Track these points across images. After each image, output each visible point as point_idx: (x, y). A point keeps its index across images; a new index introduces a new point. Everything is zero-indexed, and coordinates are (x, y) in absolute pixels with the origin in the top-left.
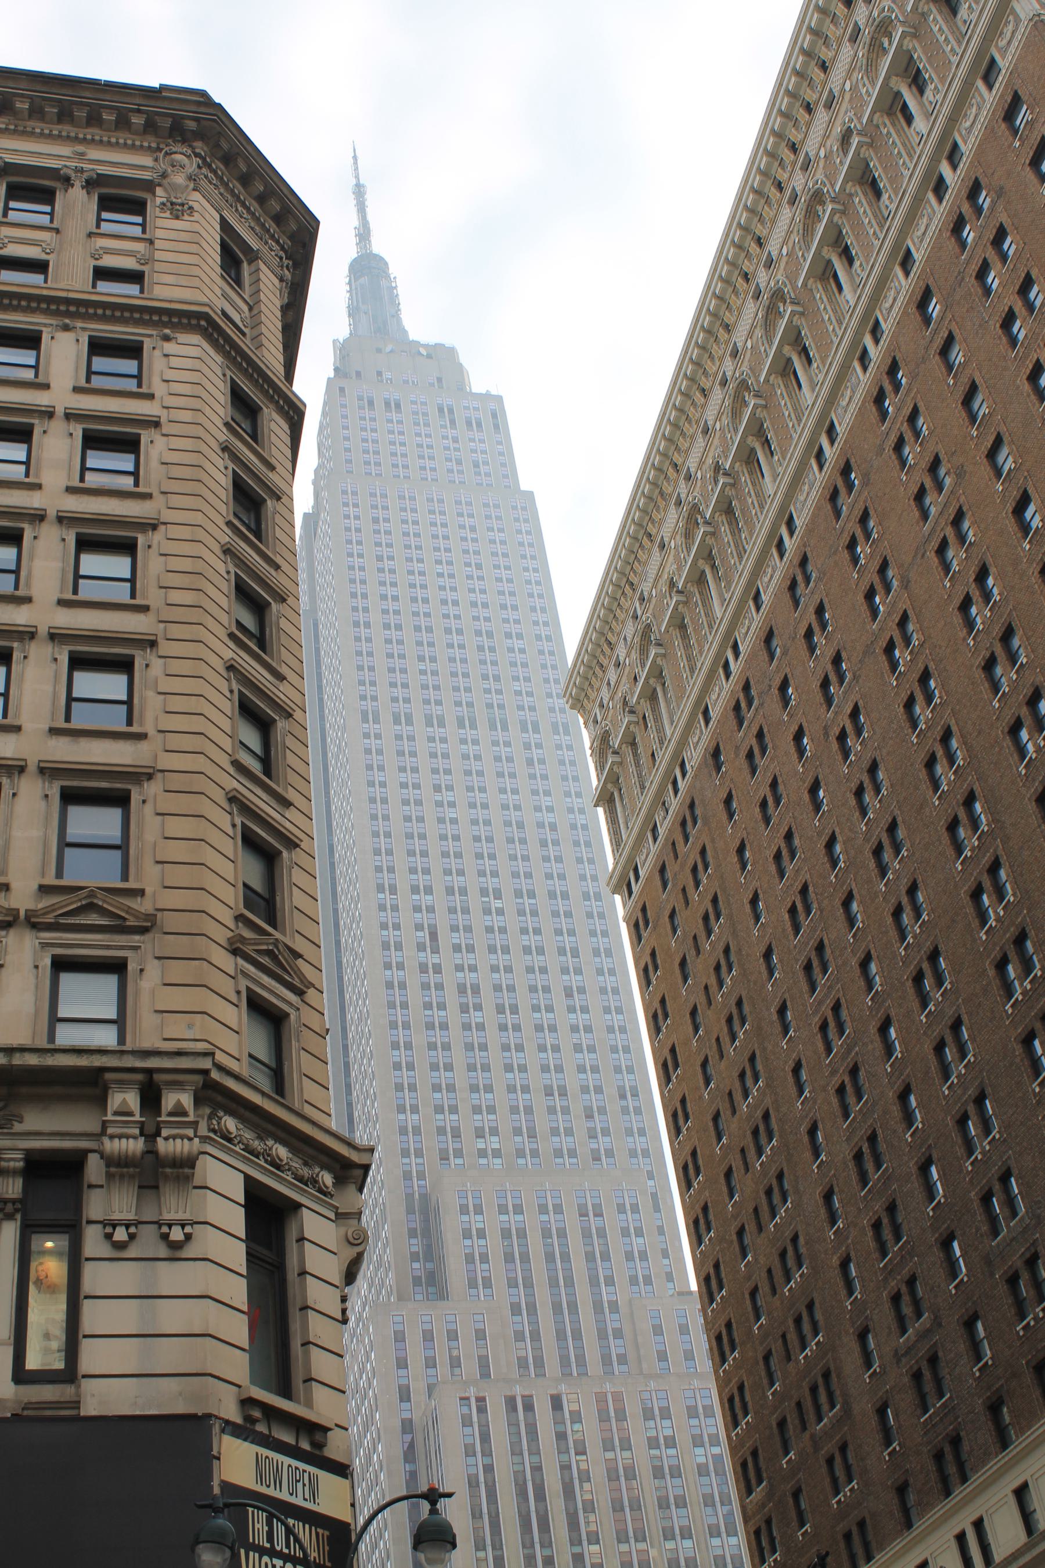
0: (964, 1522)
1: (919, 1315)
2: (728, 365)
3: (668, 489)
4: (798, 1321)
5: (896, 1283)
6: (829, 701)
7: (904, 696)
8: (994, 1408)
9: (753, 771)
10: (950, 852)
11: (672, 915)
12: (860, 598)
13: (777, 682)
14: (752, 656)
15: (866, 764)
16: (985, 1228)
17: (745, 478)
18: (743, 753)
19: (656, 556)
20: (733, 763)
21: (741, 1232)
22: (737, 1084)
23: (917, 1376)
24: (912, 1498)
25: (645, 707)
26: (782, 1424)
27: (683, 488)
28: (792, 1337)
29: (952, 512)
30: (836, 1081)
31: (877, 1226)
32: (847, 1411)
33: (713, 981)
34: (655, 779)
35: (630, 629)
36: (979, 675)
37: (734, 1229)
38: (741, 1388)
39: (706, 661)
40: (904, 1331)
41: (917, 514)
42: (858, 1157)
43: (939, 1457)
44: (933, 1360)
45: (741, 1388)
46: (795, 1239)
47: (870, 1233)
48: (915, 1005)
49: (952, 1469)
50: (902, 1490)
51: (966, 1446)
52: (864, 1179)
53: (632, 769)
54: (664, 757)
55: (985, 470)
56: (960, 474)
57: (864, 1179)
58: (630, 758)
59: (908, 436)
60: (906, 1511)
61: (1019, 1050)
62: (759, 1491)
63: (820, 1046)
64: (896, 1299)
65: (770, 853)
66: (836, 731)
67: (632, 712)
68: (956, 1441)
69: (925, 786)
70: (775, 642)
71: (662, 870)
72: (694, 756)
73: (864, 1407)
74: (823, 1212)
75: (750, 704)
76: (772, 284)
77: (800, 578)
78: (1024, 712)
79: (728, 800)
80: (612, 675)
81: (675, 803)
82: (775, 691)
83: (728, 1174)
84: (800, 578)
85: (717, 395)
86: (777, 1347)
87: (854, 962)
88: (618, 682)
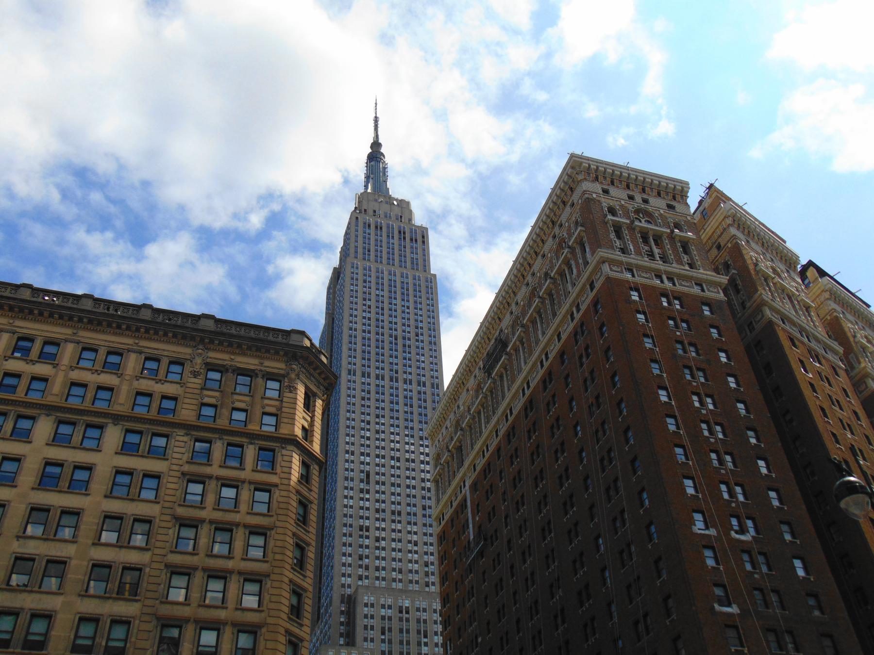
59: (551, 402)
76: (516, 313)
77: (511, 434)
84: (511, 434)
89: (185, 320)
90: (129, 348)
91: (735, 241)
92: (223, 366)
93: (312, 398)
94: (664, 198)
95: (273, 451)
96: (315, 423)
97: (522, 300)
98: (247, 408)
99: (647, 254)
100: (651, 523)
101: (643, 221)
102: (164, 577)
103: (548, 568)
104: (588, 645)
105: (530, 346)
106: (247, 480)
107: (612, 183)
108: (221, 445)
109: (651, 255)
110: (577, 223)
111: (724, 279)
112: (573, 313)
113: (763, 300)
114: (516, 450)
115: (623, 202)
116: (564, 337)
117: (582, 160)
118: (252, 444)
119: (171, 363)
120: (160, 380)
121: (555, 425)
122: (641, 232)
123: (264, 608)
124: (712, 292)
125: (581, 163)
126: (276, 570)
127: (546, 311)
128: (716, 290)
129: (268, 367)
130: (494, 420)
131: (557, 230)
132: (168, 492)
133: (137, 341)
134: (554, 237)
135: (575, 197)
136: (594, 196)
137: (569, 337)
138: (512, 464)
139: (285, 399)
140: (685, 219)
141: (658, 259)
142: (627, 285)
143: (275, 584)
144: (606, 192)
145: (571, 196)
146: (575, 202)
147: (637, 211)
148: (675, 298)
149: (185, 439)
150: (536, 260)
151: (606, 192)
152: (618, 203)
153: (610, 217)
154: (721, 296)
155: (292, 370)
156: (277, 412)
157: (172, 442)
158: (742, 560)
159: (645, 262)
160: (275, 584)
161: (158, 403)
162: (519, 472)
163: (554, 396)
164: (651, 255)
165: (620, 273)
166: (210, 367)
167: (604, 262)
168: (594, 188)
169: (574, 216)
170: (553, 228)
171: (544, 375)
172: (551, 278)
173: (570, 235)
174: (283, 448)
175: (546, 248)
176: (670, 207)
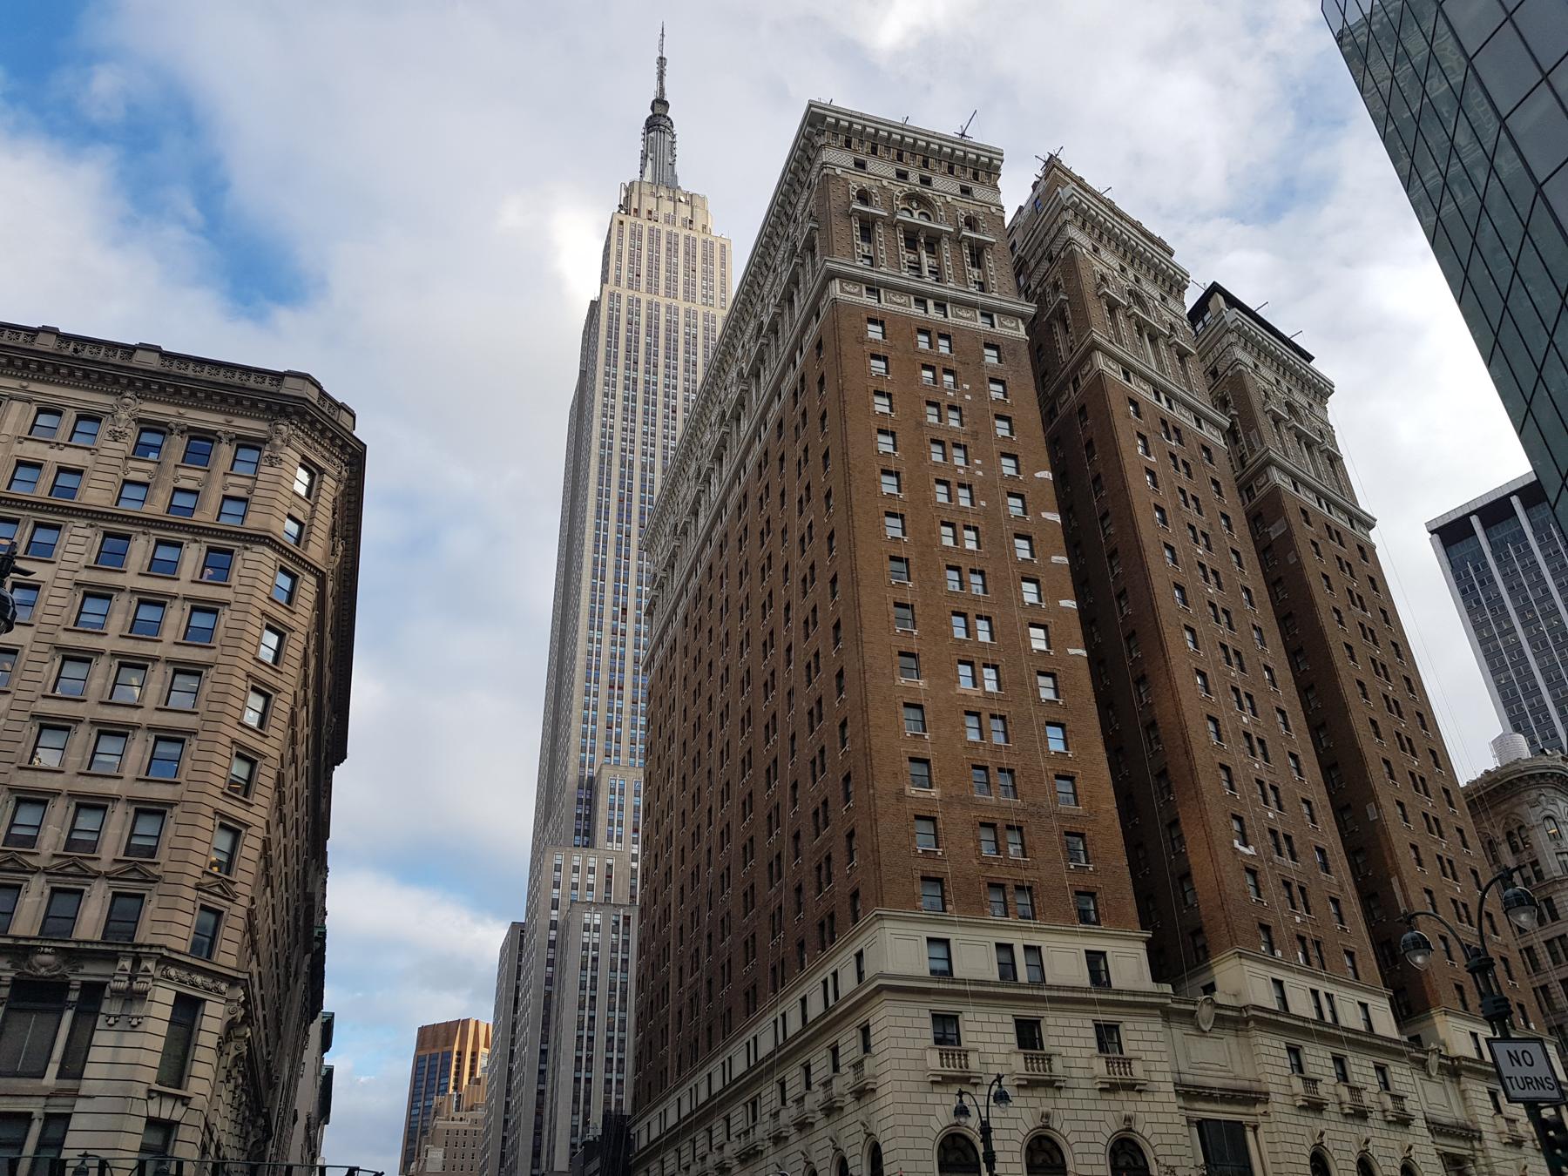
89: (111, 353)
90: (10, 394)
91: (1070, 248)
92: (165, 424)
93: (317, 477)
94: (958, 177)
95: (231, 552)
98: (198, 488)
99: (909, 267)
101: (916, 214)
102: (28, 733)
106: (181, 596)
108: (145, 542)
109: (916, 268)
111: (1030, 309)
113: (1094, 341)
115: (885, 183)
117: (826, 112)
118: (196, 541)
119: (80, 418)
120: (58, 444)
123: (182, 779)
124: (1006, 327)
125: (825, 117)
126: (209, 726)
128: (1013, 325)
132: (49, 610)
133: (25, 384)
136: (839, 171)
139: (261, 477)
140: (986, 210)
141: (927, 274)
142: (864, 316)
143: (204, 746)
144: (860, 165)
147: (909, 197)
148: (943, 336)
149: (88, 532)
151: (860, 165)
152: (878, 183)
154: (1022, 333)
155: (279, 432)
158: (963, 724)
159: (905, 278)
160: (204, 746)
161: (52, 478)
164: (916, 268)
165: (858, 295)
167: (833, 278)
168: (836, 158)
174: (247, 549)
176: (966, 191)
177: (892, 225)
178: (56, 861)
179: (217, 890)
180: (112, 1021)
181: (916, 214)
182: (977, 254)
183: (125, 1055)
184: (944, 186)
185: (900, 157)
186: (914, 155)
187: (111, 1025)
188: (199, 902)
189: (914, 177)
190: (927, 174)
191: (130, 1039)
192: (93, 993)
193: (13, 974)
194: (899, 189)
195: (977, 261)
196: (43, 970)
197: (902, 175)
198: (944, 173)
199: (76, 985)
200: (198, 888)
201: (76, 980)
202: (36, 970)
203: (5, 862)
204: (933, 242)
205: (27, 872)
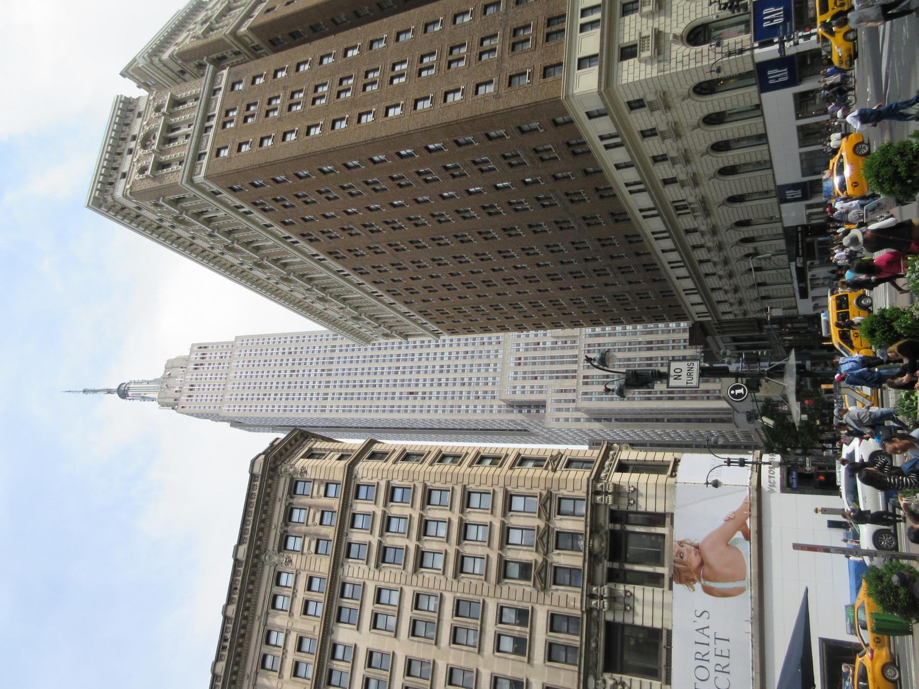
0: (668, 267)
1: (605, 270)
2: (272, 281)
3: (307, 305)
4: (596, 302)
5: (594, 275)
6: (405, 268)
7: (415, 249)
8: (638, 254)
9: (418, 292)
10: (470, 243)
11: (454, 322)
12: (376, 256)
13: (392, 282)
14: (379, 288)
15: (432, 262)
16: (586, 250)
17: (316, 282)
18: (411, 295)
19: (328, 312)
20: (413, 298)
21: (564, 314)
22: (517, 310)
23: (623, 273)
24: (658, 278)
25: (380, 321)
26: (626, 310)
27: (308, 301)
28: (601, 304)
29: (362, 227)
30: (527, 283)
31: (575, 277)
32: (626, 292)
33: (481, 313)
34: (407, 321)
35: (350, 323)
36: (419, 228)
37: (562, 316)
38: (612, 320)
39: (374, 301)
40: (609, 274)
41: (357, 237)
42: (552, 280)
43: (648, 270)
44: (620, 268)
45: (612, 320)
46: (571, 300)
47: (577, 280)
48: (513, 259)
49: (652, 267)
50: (654, 280)
51: (647, 263)
52: (561, 279)
53: (400, 328)
54: (401, 317)
55: (353, 217)
56: (350, 223)
57: (561, 279)
58: (396, 328)
59: (329, 235)
60: (661, 280)
61: (537, 235)
62: (644, 318)
63: (514, 285)
64: (598, 275)
65: (447, 292)
66: (416, 268)
67: (380, 326)
68: (645, 265)
69: (446, 247)
70: (377, 281)
71: (438, 323)
72: (404, 309)
73: (628, 287)
74: (566, 291)
75: (395, 291)
78: (436, 219)
79: (424, 301)
80: (363, 330)
81: (417, 317)
82: (394, 283)
83: (544, 315)
85: (281, 286)
86: (602, 308)
87: (493, 273)
88: (367, 328)
96: (336, 448)
97: (237, 259)
100: (427, 148)
103: (471, 241)
104: (531, 208)
105: (279, 253)
107: (115, 169)
110: (156, 205)
112: (244, 212)
114: (374, 267)
115: (135, 160)
116: (268, 222)
121: (349, 232)
122: (164, 144)
125: (95, 197)
127: (246, 237)
129: (283, 494)
130: (349, 286)
131: (166, 224)
134: (173, 227)
135: (131, 205)
136: (128, 186)
137: (269, 217)
138: (386, 271)
145: (130, 209)
146: (135, 205)
150: (198, 245)
153: (148, 173)
156: (324, 485)
157: (348, 579)
162: (393, 265)
163: (323, 232)
166: (283, 548)
168: (121, 187)
169: (149, 207)
170: (165, 228)
171: (305, 241)
172: (213, 232)
173: (169, 212)
175: (186, 235)
177: (161, 152)
178: (540, 549)
179: (556, 463)
180: (632, 502)
181: (153, 141)
182: (176, 103)
183: (651, 491)
184: (138, 127)
185: (119, 154)
186: (119, 146)
187: (634, 502)
188: (563, 469)
189: (132, 145)
190: (130, 138)
191: (642, 490)
192: (617, 516)
193: (605, 562)
194: (141, 152)
195: (182, 102)
196: (603, 545)
197: (130, 151)
198: (130, 128)
199: (611, 526)
200: (555, 470)
201: (608, 526)
202: (603, 548)
203: (541, 578)
204: (171, 128)
205: (547, 564)
